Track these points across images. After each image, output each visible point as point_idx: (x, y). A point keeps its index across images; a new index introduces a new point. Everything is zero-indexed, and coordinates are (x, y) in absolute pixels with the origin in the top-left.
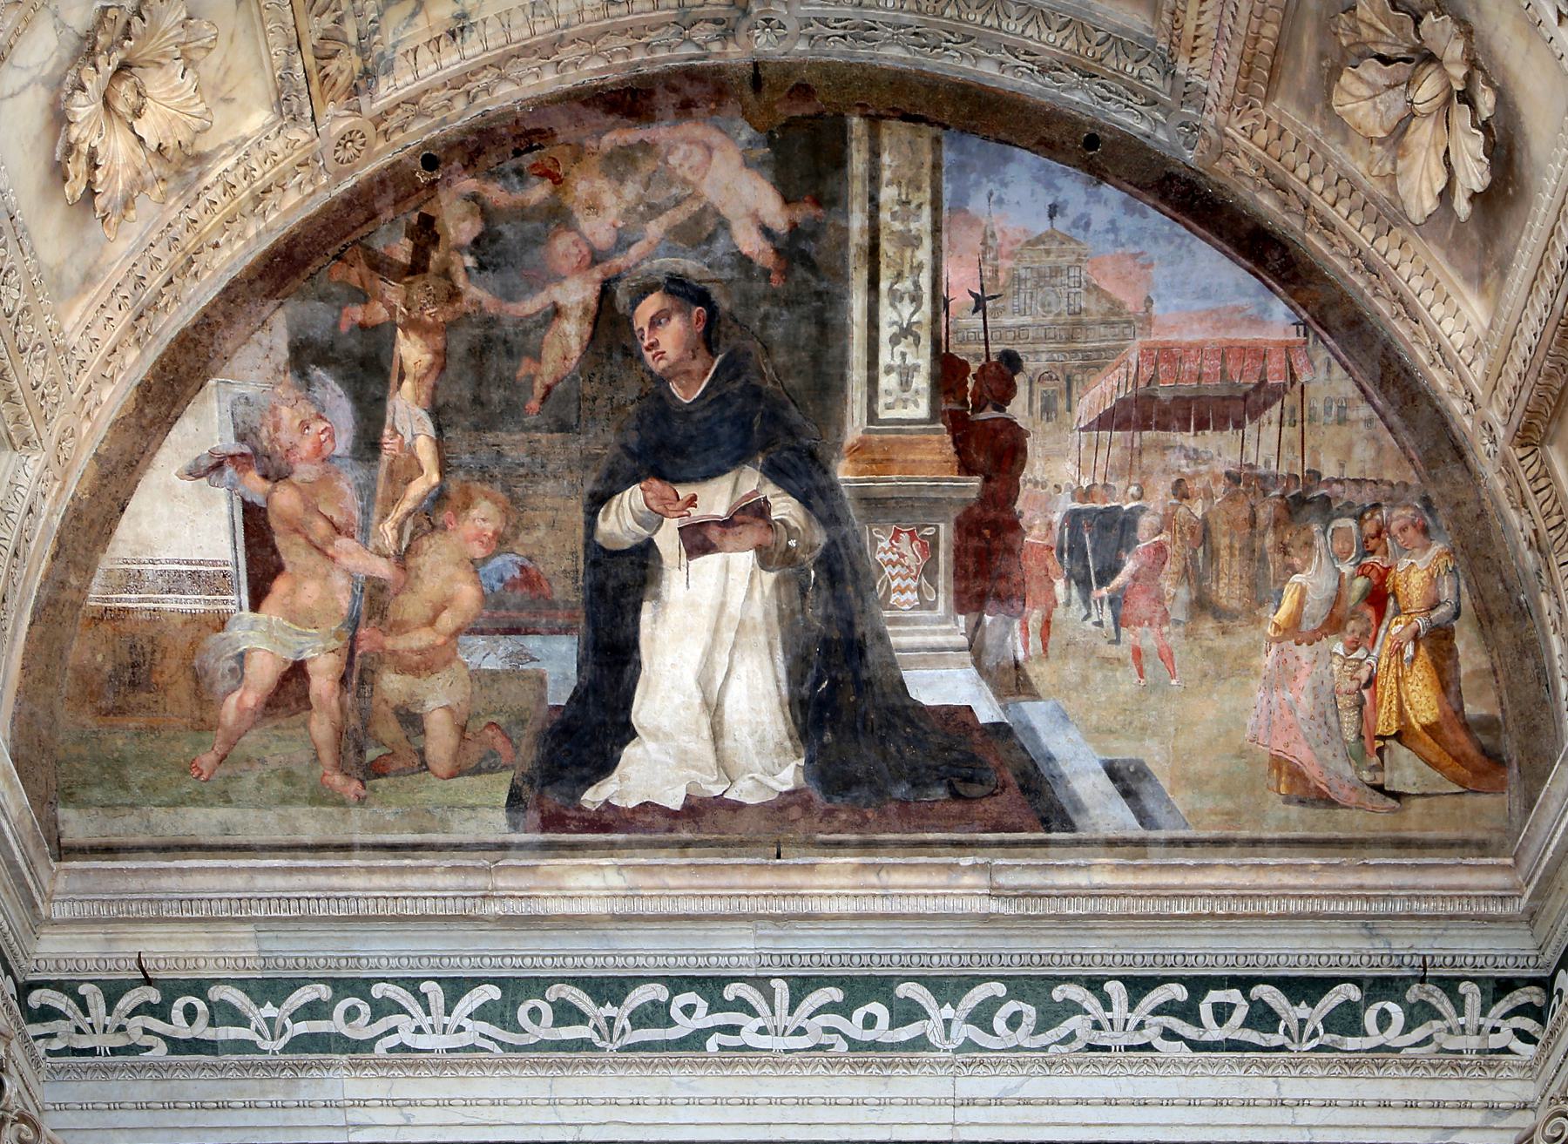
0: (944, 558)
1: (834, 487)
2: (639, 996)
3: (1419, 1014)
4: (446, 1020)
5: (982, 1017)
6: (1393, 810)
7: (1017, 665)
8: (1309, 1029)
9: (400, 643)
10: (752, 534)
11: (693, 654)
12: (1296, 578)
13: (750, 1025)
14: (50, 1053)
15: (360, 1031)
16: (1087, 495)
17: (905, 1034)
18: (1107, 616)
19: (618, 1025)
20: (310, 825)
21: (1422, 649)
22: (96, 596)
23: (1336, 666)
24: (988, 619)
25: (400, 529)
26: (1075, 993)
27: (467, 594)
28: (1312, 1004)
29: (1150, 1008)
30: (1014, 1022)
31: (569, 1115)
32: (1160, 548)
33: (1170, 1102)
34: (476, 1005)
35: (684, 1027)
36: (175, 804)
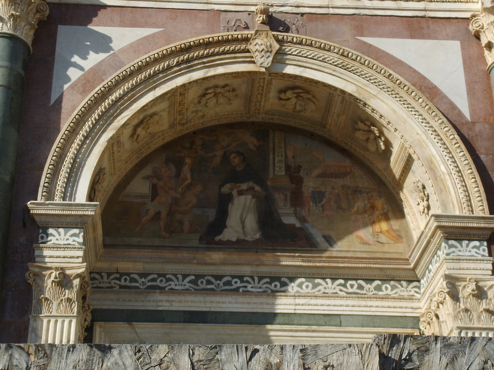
0: (288, 198)
2: (225, 279)
4: (182, 283)
6: (382, 246)
7: (304, 217)
8: (371, 290)
12: (357, 204)
13: (250, 286)
15: (163, 285)
18: (321, 209)
19: (220, 285)
20: (157, 242)
21: (383, 217)
23: (366, 219)
24: (298, 208)
28: (371, 284)
29: (337, 284)
31: (208, 305)
34: (189, 280)
35: (235, 286)
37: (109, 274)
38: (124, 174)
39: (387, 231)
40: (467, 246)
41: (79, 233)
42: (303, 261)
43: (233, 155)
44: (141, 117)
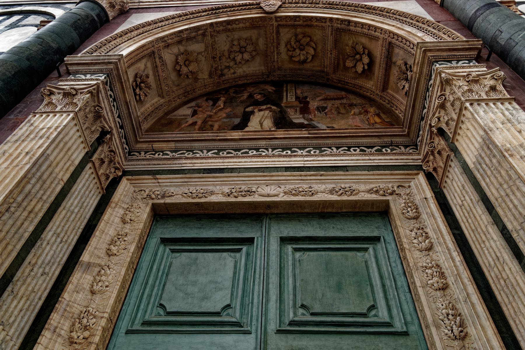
1: (282, 106)
9: (213, 120)
10: (270, 109)
11: (259, 119)
18: (324, 114)
22: (168, 117)
42: (309, 134)
43: (257, 95)
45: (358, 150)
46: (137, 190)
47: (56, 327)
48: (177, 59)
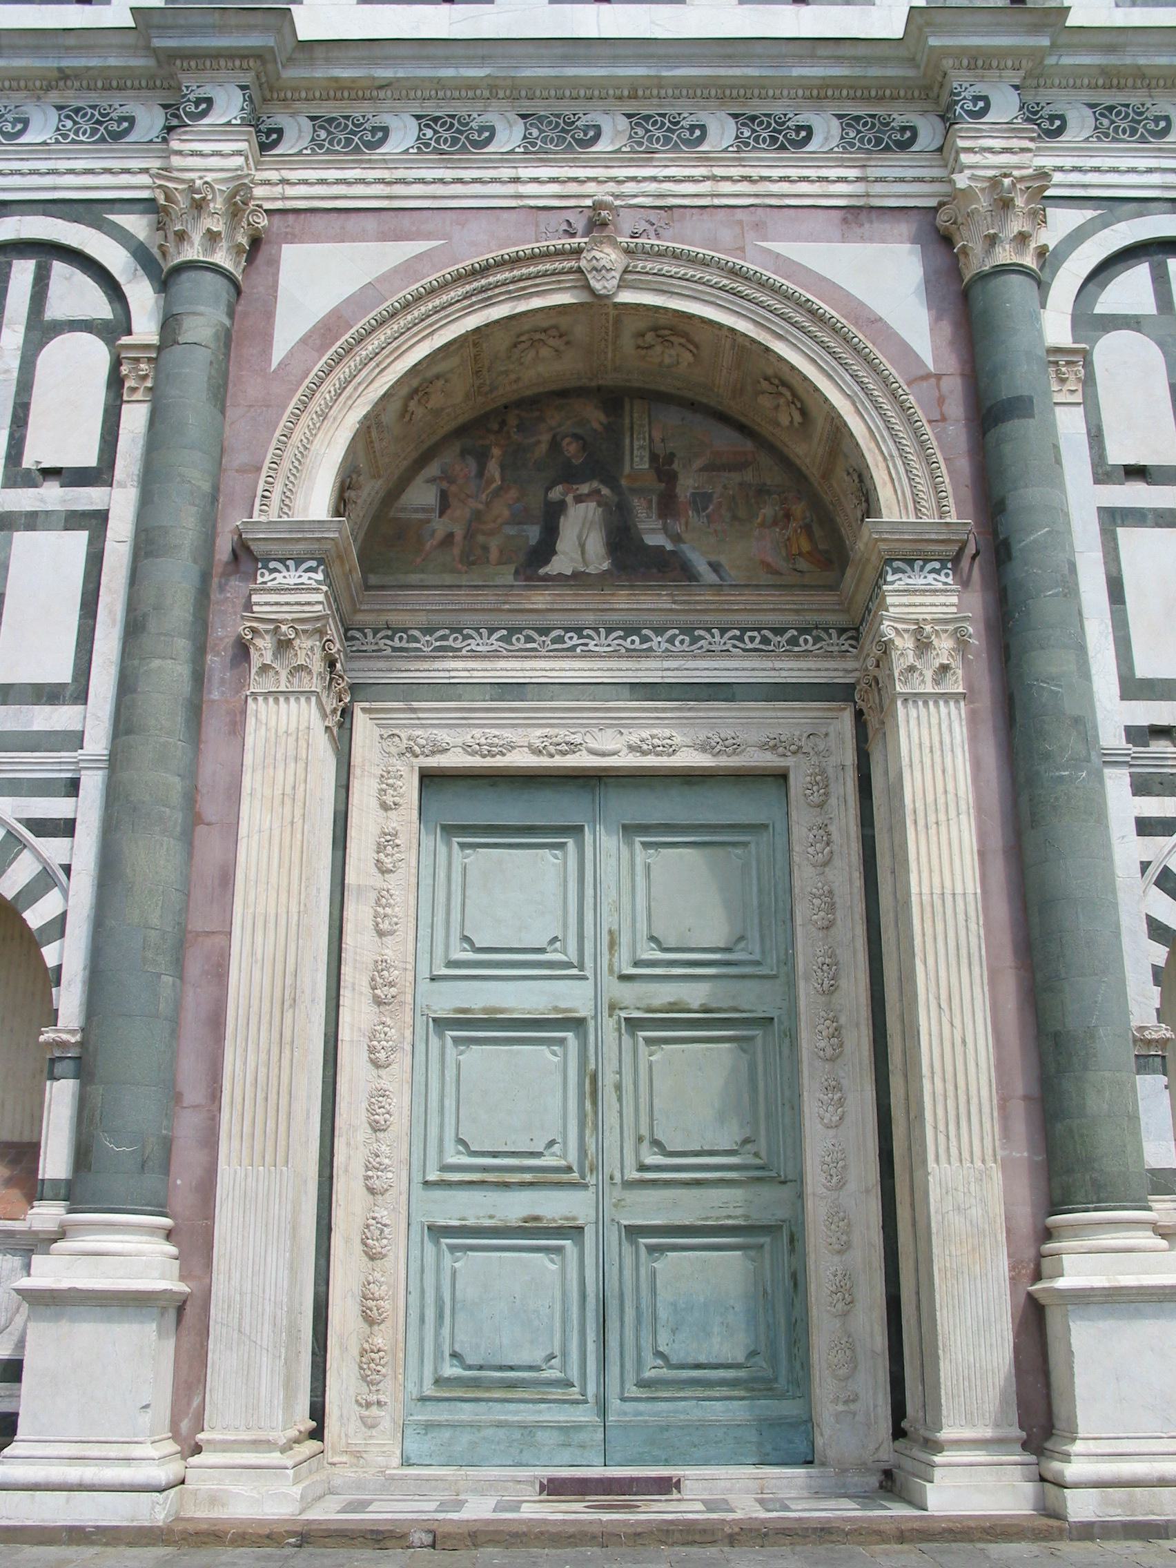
3: (817, 640)
5: (671, 641)
11: (576, 531)
14: (352, 651)
15: (458, 645)
16: (695, 488)
17: (645, 646)
20: (448, 579)
22: (392, 514)
25: (487, 495)
26: (702, 633)
27: (506, 513)
30: (682, 642)
32: (720, 503)
33: (737, 669)
35: (569, 644)
36: (406, 573)
37: (376, 631)
38: (396, 477)
39: (808, 553)
40: (922, 569)
41: (318, 566)
43: (567, 440)
44: (415, 383)
45: (757, 640)
46: (386, 733)
47: (354, 984)
48: (406, 406)
